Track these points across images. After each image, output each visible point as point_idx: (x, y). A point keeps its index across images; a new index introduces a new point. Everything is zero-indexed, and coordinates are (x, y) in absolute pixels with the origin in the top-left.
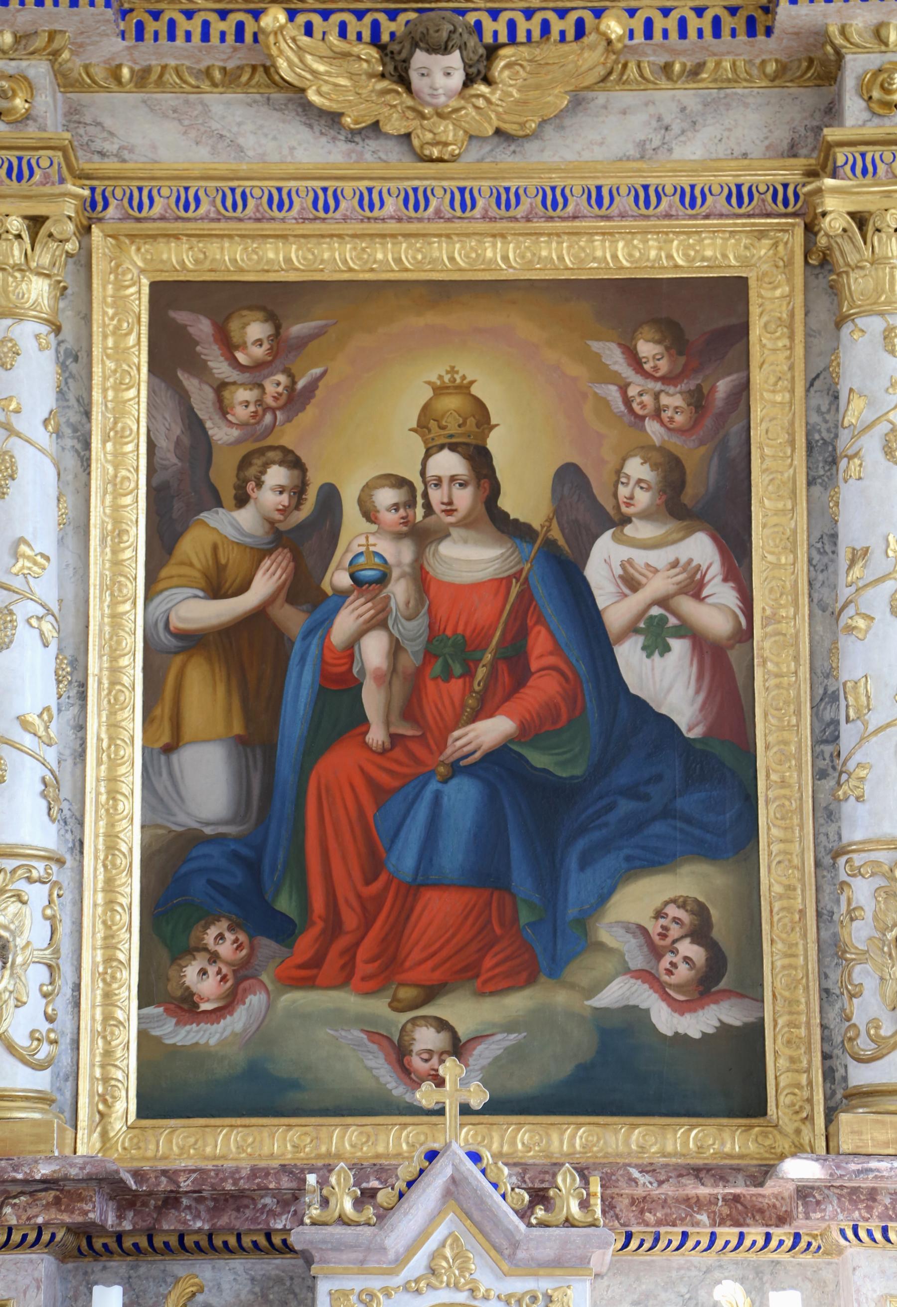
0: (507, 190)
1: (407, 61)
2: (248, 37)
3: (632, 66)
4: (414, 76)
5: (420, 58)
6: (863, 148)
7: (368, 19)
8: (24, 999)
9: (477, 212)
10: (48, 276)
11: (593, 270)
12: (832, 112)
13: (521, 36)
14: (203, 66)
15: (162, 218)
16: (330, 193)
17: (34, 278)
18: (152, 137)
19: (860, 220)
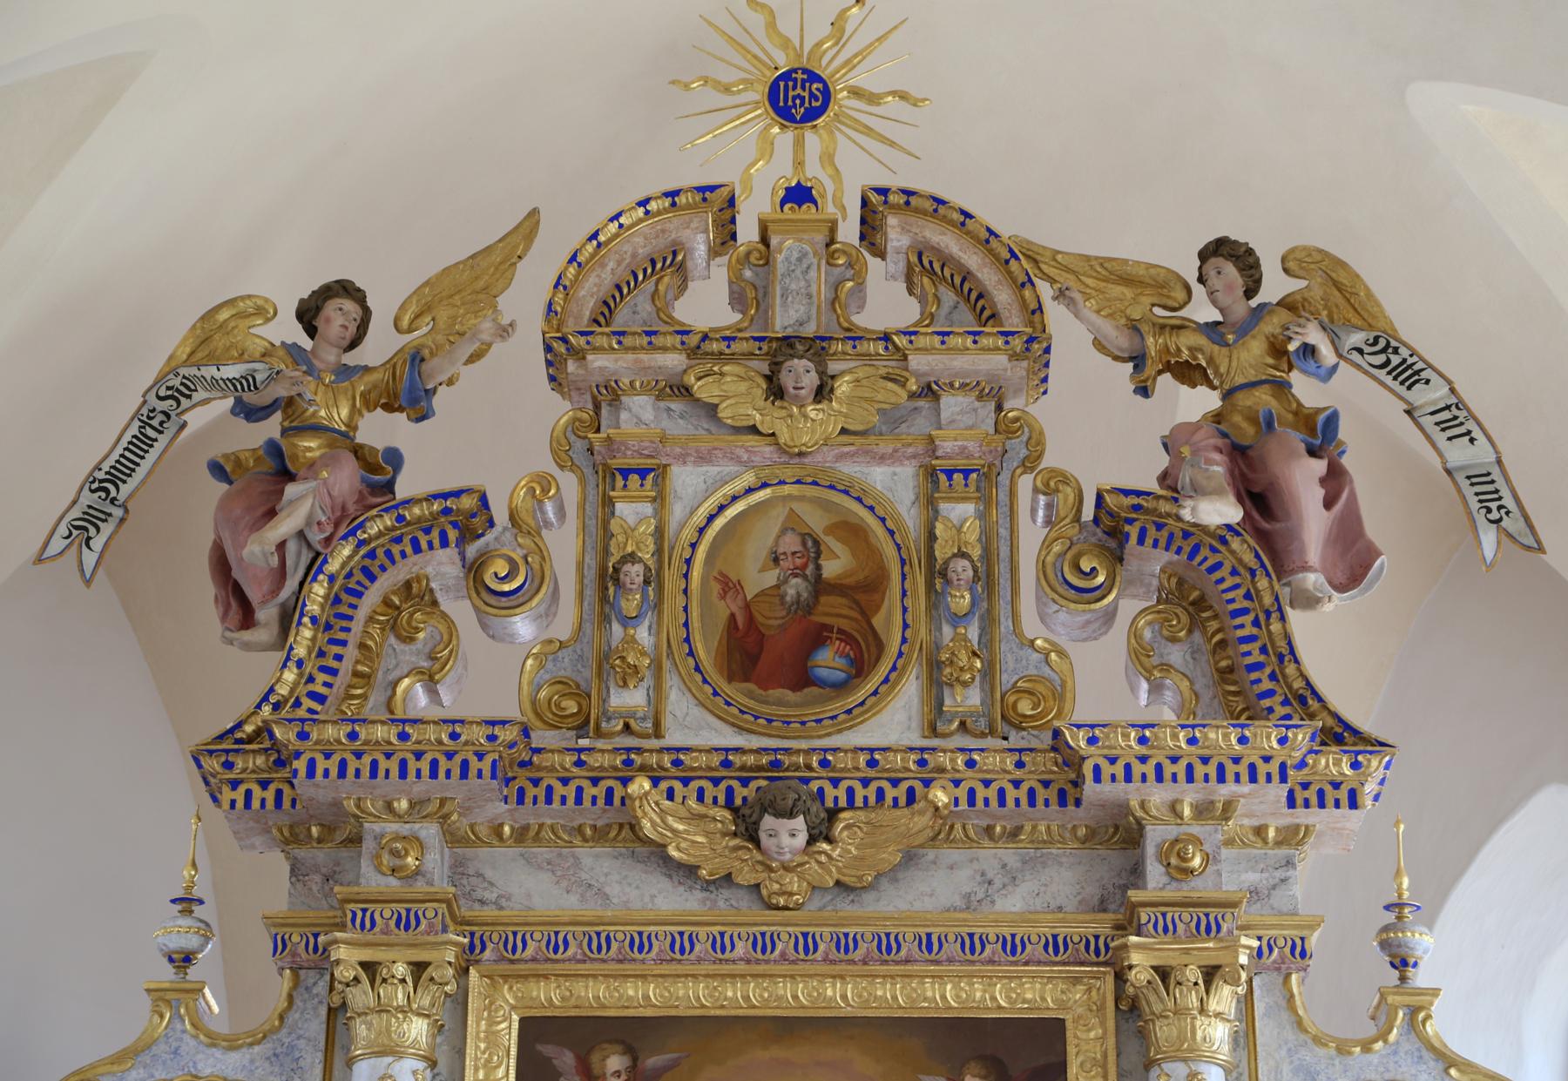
0: (846, 935)
1: (757, 823)
2: (617, 801)
3: (958, 826)
4: (763, 836)
5: (768, 821)
6: (1163, 909)
7: (723, 785)
9: (819, 956)
10: (428, 1016)
11: (924, 1010)
12: (1136, 873)
13: (859, 802)
14: (576, 824)
15: (534, 960)
16: (686, 937)
17: (415, 1019)
18: (527, 887)
19: (1163, 973)
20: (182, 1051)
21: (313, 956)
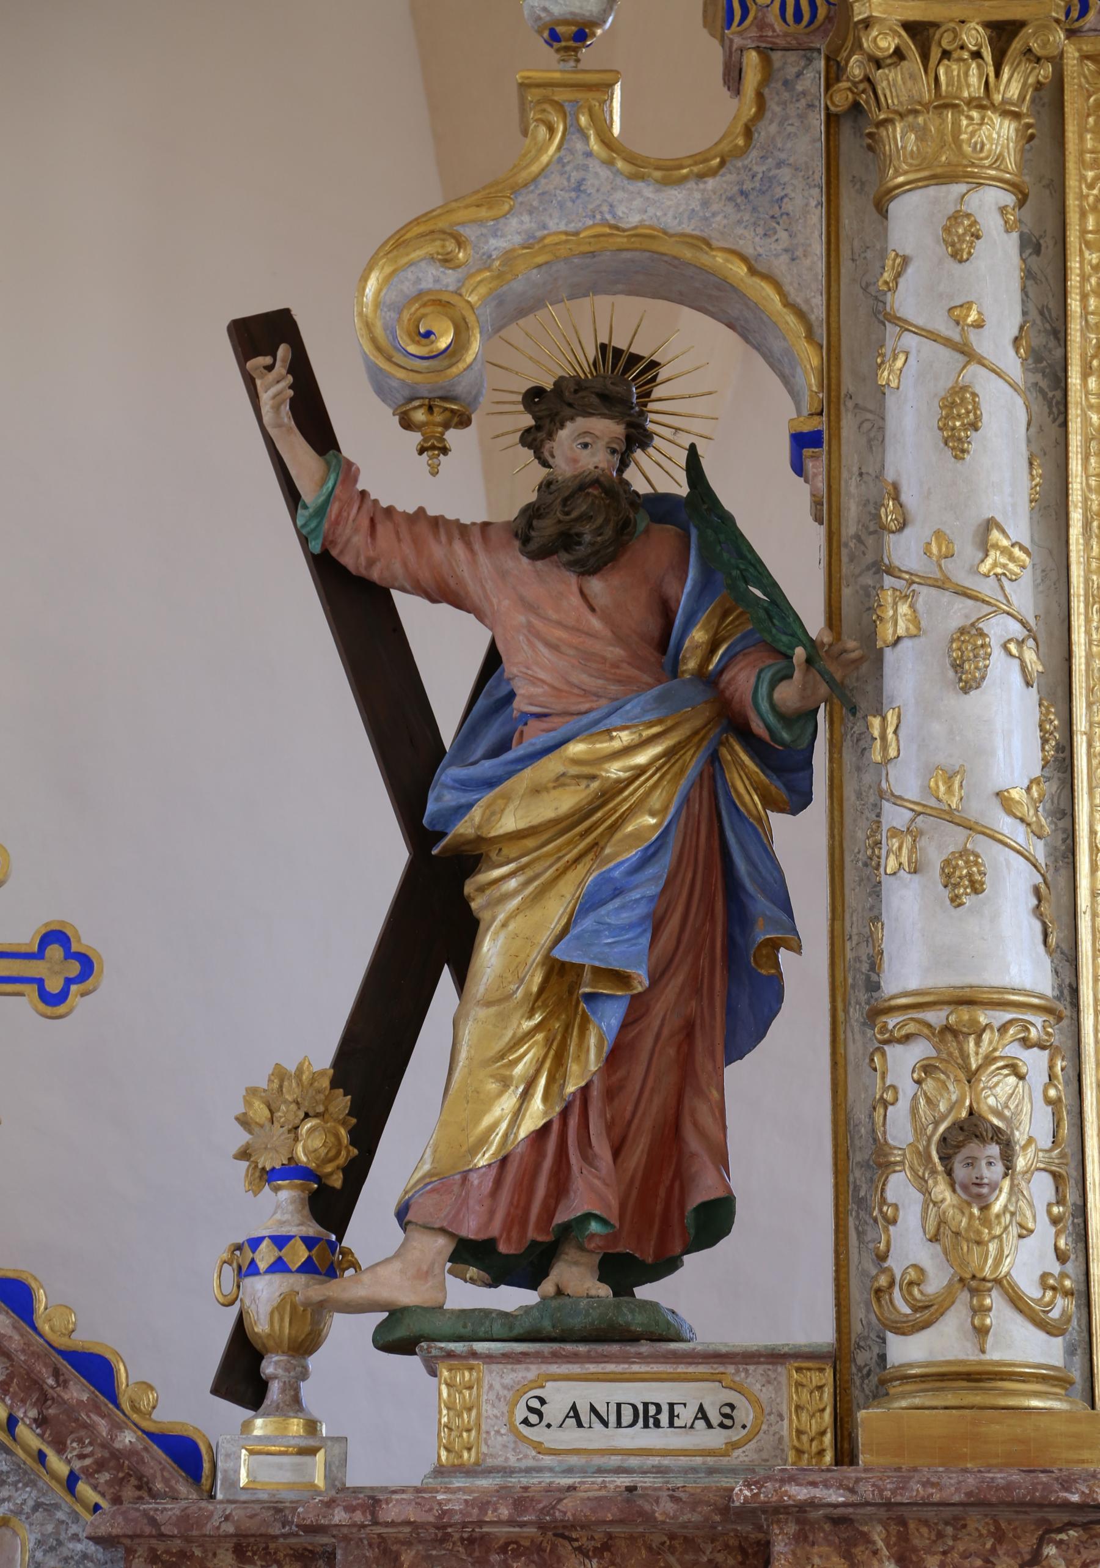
8: (1030, 1225)
10: (1016, 116)
17: (997, 120)
20: (590, 184)
21: (793, 28)
